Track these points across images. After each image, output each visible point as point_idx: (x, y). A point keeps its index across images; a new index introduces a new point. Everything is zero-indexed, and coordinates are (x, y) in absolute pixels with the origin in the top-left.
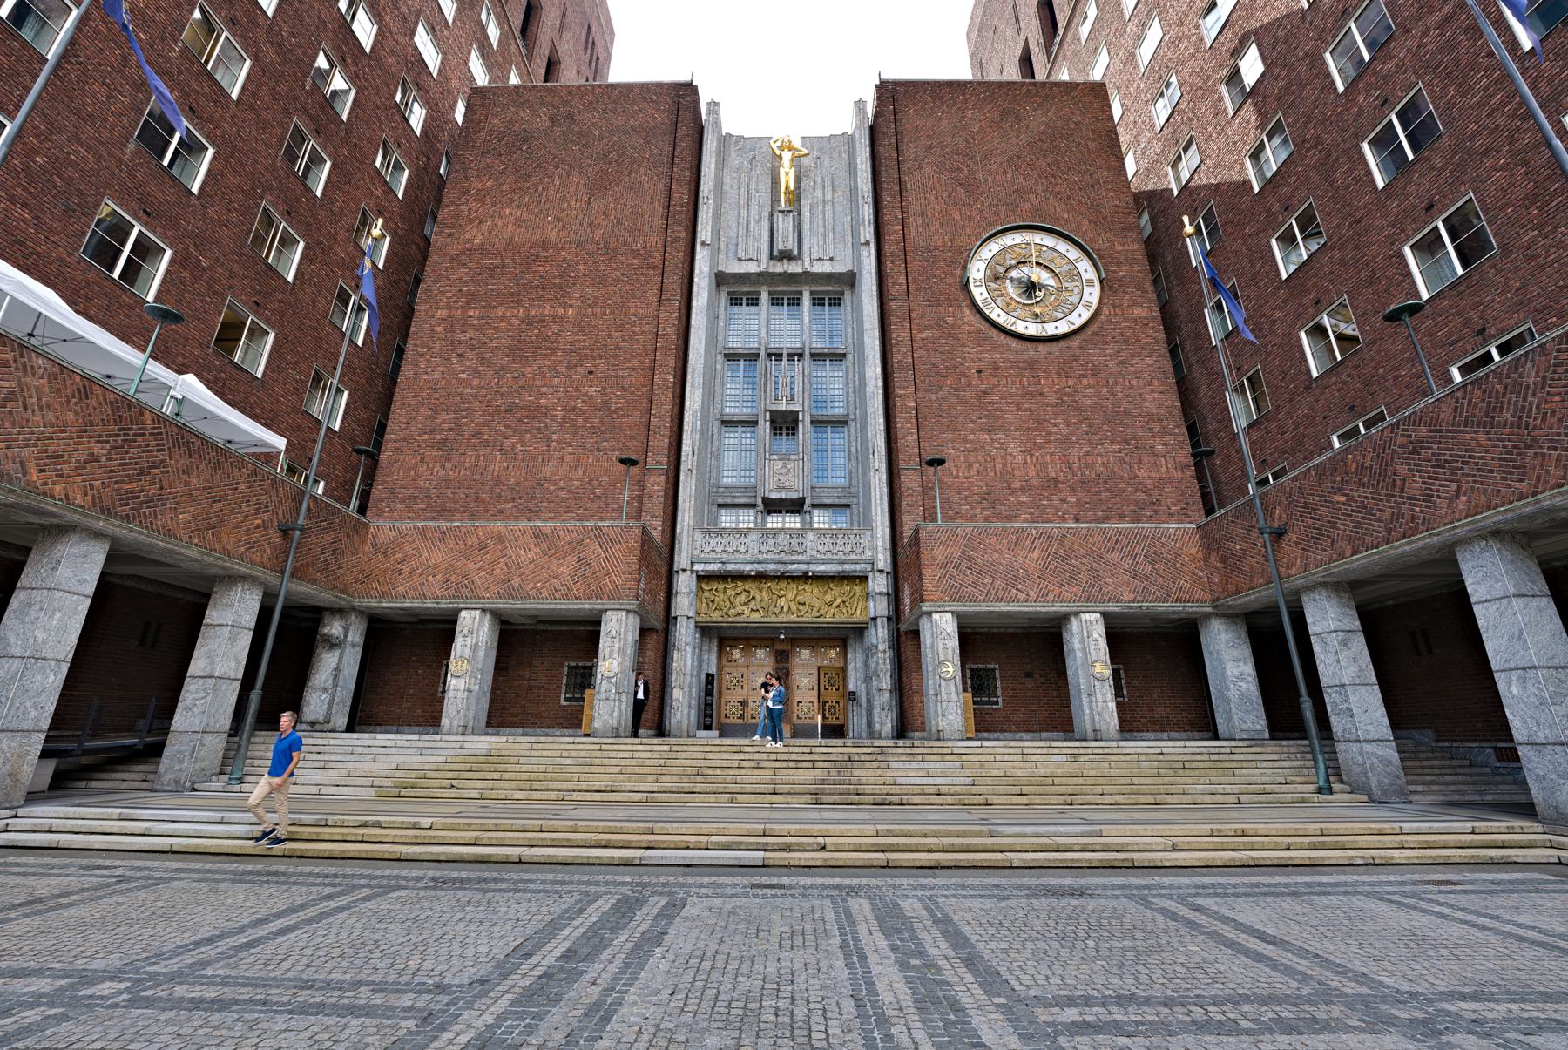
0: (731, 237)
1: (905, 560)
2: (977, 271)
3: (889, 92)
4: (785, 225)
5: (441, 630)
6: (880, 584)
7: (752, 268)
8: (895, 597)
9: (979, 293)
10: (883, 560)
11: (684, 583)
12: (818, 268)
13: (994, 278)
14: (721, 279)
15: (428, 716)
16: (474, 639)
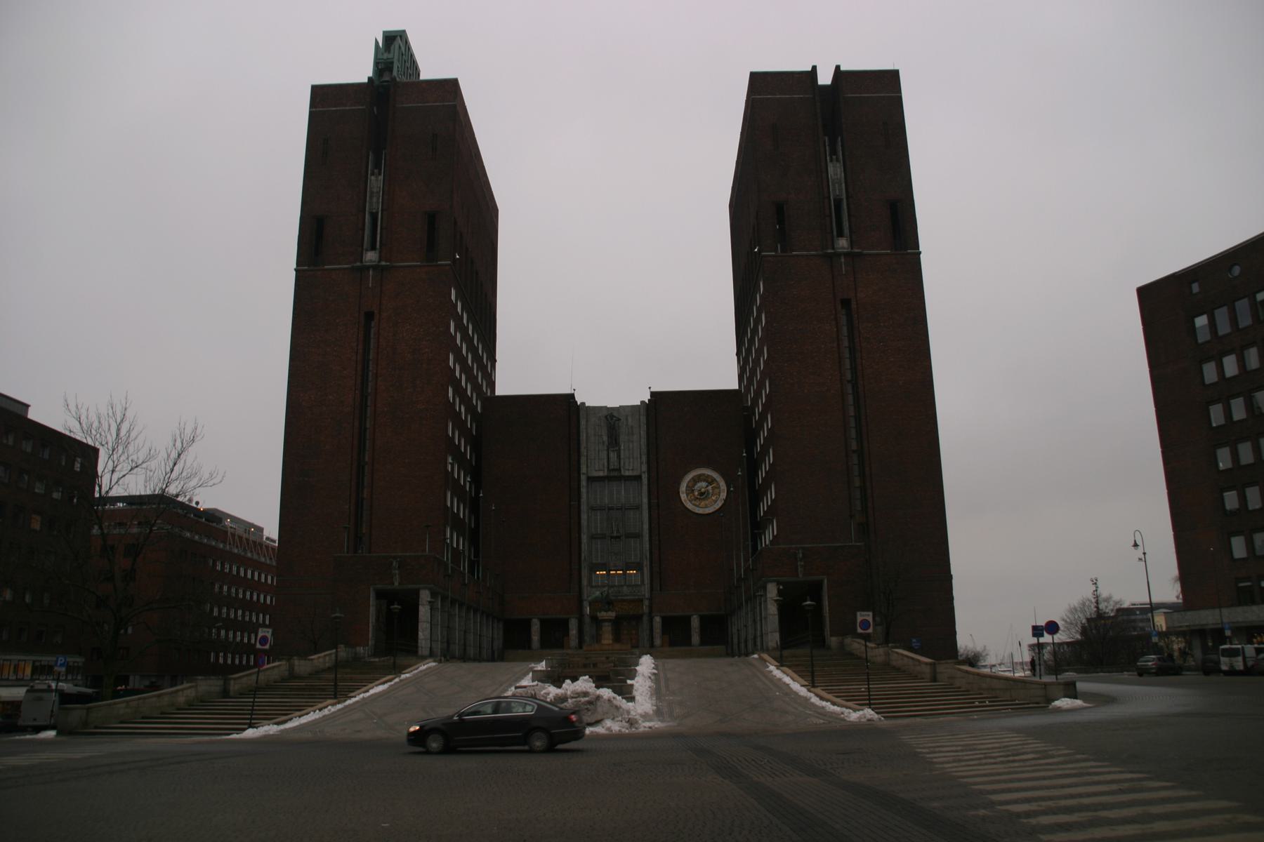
0: (594, 461)
1: (650, 599)
2: (683, 487)
3: (653, 394)
4: (613, 456)
5: (527, 624)
6: (646, 603)
7: (601, 474)
8: (651, 607)
9: (683, 497)
10: (647, 595)
11: (586, 604)
12: (627, 473)
13: (690, 490)
14: (591, 479)
15: (527, 644)
16: (536, 627)
